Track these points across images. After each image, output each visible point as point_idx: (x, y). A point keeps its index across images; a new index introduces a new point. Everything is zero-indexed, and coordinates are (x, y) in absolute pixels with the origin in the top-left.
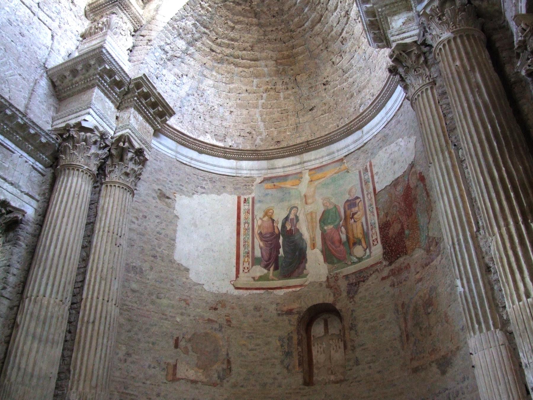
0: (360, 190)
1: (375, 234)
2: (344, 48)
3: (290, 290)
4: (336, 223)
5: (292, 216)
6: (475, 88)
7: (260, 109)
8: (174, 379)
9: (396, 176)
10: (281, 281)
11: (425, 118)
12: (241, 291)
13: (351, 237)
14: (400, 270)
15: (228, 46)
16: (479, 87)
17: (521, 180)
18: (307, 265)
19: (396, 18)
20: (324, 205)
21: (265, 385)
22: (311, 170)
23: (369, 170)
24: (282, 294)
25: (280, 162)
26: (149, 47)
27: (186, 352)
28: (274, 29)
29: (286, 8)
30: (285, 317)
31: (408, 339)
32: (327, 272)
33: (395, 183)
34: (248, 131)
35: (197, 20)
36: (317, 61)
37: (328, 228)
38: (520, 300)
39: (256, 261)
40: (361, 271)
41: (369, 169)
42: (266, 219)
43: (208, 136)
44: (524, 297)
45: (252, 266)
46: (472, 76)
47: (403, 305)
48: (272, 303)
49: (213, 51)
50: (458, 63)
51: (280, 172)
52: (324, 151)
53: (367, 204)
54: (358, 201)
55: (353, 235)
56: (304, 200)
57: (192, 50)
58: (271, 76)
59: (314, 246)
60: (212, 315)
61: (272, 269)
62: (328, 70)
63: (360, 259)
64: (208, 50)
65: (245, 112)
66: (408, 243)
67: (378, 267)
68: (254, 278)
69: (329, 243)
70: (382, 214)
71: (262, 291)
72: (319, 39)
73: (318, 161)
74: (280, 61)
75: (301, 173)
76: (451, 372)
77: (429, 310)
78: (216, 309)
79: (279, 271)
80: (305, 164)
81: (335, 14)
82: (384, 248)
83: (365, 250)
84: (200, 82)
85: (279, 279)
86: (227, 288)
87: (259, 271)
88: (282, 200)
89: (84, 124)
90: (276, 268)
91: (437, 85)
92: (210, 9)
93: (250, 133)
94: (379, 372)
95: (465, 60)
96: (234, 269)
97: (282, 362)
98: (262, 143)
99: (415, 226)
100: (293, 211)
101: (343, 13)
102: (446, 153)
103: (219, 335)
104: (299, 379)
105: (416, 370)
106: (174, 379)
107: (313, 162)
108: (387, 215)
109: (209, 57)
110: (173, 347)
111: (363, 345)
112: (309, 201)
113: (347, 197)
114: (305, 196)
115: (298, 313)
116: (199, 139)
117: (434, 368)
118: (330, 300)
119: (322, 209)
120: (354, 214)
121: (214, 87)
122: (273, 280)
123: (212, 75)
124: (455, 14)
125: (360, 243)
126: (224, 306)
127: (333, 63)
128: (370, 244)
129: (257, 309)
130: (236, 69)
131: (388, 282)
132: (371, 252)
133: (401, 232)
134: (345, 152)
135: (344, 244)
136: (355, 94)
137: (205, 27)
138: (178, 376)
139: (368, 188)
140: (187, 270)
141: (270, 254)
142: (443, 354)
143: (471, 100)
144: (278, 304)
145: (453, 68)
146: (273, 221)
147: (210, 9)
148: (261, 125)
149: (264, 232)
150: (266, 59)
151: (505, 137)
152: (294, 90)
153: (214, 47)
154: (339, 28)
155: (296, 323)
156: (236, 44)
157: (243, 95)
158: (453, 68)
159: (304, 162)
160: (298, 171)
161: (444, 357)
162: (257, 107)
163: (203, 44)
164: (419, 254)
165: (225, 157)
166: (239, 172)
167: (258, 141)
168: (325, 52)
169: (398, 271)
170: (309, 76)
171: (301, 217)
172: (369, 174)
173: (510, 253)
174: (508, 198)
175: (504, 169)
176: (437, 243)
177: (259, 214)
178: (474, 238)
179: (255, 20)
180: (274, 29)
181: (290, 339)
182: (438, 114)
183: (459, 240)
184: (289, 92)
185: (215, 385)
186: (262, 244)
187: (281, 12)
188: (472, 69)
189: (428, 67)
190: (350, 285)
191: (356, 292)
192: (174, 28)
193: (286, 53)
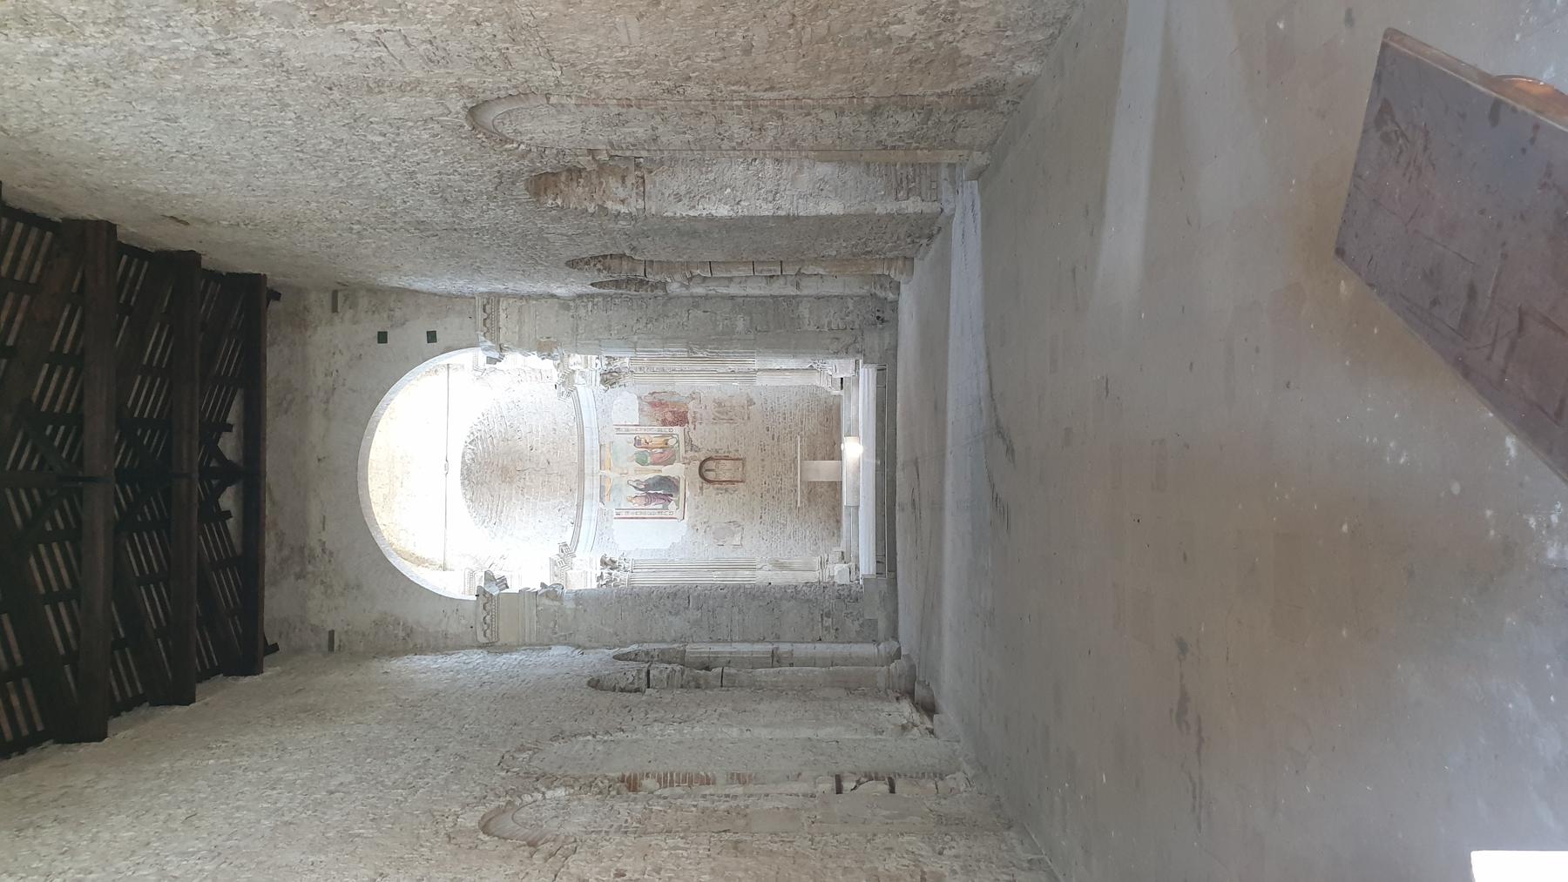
0: (629, 436)
1: (666, 429)
5: (635, 484)
8: (741, 545)
13: (660, 446)
14: (694, 418)
15: (491, 513)
19: (576, 381)
20: (632, 461)
21: (744, 504)
25: (587, 491)
33: (641, 410)
36: (513, 450)
42: (634, 502)
47: (714, 419)
60: (701, 532)
63: (678, 442)
64: (495, 526)
70: (655, 423)
76: (755, 400)
87: (672, 506)
88: (620, 490)
89: (599, 575)
90: (672, 496)
93: (559, 510)
99: (675, 404)
103: (713, 527)
104: (741, 484)
112: (625, 472)
117: (750, 408)
118: (698, 463)
131: (698, 426)
139: (632, 430)
164: (691, 405)
177: (630, 505)
181: (717, 489)
184: (527, 479)
185: (743, 529)
187: (480, 463)
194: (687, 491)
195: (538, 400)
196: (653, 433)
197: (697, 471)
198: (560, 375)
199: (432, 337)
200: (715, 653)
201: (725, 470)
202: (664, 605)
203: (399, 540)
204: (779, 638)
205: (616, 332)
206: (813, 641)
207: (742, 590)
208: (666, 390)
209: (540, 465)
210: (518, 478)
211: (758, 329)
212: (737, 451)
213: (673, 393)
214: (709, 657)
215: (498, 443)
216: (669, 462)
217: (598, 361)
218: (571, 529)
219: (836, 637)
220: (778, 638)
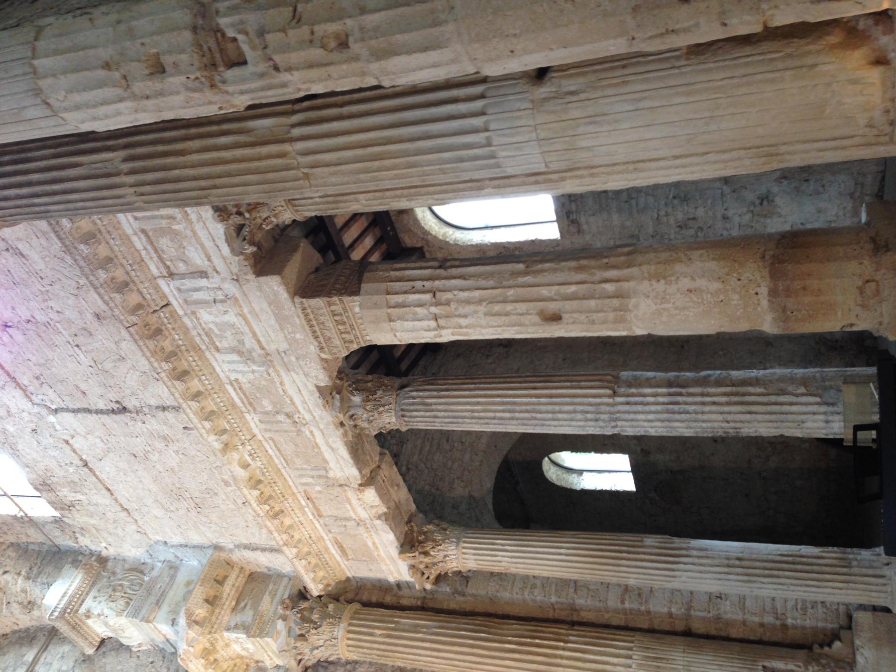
6: (415, 629)
16: (418, 626)
46: (402, 627)
50: (378, 632)
175: (510, 638)
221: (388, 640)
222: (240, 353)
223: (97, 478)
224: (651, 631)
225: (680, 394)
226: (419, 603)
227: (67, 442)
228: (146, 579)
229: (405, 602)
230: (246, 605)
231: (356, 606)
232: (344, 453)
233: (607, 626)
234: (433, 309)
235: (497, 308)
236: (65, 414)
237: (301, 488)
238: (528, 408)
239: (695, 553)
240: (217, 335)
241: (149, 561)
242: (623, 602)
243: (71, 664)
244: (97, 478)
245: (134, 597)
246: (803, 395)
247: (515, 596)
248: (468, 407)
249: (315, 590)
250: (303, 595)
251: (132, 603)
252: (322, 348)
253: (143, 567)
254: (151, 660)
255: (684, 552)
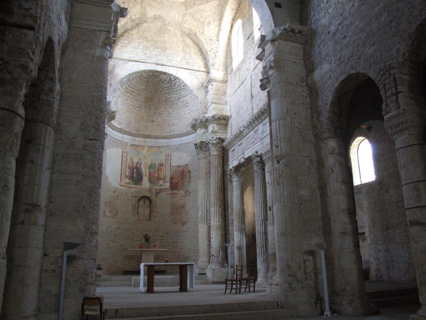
0: (165, 161)
1: (168, 179)
2: (172, 106)
3: (137, 189)
4: (155, 170)
5: (139, 162)
6: (218, 172)
7: (134, 114)
8: (105, 216)
9: (180, 164)
10: (134, 186)
11: (202, 166)
12: (121, 187)
13: (159, 177)
14: (174, 194)
15: (132, 88)
17: (221, 198)
18: (143, 181)
19: (202, 129)
22: (148, 146)
23: (170, 156)
24: (134, 190)
25: (138, 139)
26: (111, 88)
27: (107, 207)
28: (151, 88)
29: (159, 85)
30: (134, 198)
31: (173, 214)
32: (149, 186)
33: (179, 166)
34: (128, 122)
35: (128, 79)
37: (152, 171)
38: (215, 223)
39: (127, 177)
40: (161, 189)
41: (169, 155)
42: (131, 161)
43: (116, 123)
44: (216, 223)
45: (126, 178)
47: (174, 204)
48: (130, 192)
49: (126, 88)
50: (216, 163)
51: (137, 143)
52: (154, 140)
53: (167, 168)
54: (163, 165)
55: (160, 176)
56: (144, 157)
57: (121, 87)
58: (141, 102)
59: (146, 175)
60: (113, 194)
61: (131, 180)
62: (163, 109)
63: (161, 185)
64: (125, 88)
65: (129, 114)
66: (179, 187)
67: (167, 190)
68: (125, 183)
69: (151, 176)
70: (172, 174)
71: (128, 188)
72: (165, 98)
73: (151, 144)
74: (147, 98)
75: (144, 146)
77: (182, 209)
78: (114, 192)
79: (133, 181)
80: (146, 143)
81: (175, 95)
82: (170, 185)
83: (163, 183)
84: (118, 99)
85: (133, 185)
86: (117, 185)
87: (127, 180)
90: (133, 180)
91: (207, 159)
92: (134, 77)
94: (162, 221)
95: (218, 163)
96: (120, 179)
97: (132, 213)
98: (132, 129)
100: (140, 161)
101: (178, 97)
102: (205, 180)
105: (174, 223)
106: (105, 216)
107: (149, 143)
108: (173, 175)
109: (124, 90)
110: (104, 205)
111: (158, 212)
112: (146, 158)
113: (160, 162)
114: (145, 156)
115: (138, 197)
116: (114, 124)
117: (180, 223)
118: (149, 195)
119: (150, 163)
120: (161, 169)
121: (121, 101)
122: (131, 184)
123: (122, 97)
124: (219, 148)
125: (162, 180)
126: (116, 192)
127: (166, 108)
128: (165, 181)
129: (126, 194)
130: (131, 96)
131: (169, 196)
132: (165, 184)
133: (178, 183)
134: (162, 145)
135: (156, 178)
136: (171, 125)
137: (129, 81)
138: (106, 215)
139: (168, 162)
140: (108, 178)
141: (131, 175)
142: (184, 221)
143: (217, 175)
144: (132, 193)
145: (215, 164)
146: (133, 162)
147: (134, 77)
148: (133, 121)
149: (130, 166)
150: (142, 96)
151: (221, 188)
152: (148, 111)
153: (128, 88)
154: (174, 100)
155: (137, 201)
156: (135, 88)
157: (130, 106)
158: (215, 164)
159: (146, 142)
160: (144, 145)
161: (184, 222)
162: (133, 113)
163: (125, 86)
164: (182, 192)
165: (120, 132)
166: (124, 139)
167: (131, 128)
168: (165, 103)
169: (174, 194)
170: (155, 108)
171: (143, 164)
172: (170, 158)
173: (215, 213)
174: (218, 202)
176: (190, 193)
178: (206, 203)
179: (146, 83)
180: (151, 88)
182: (205, 167)
183: (203, 203)
184: (146, 111)
185: (113, 218)
186: (129, 170)
187: (157, 85)
188: (219, 167)
189: (206, 151)
190: (156, 192)
191: (158, 195)
192: (121, 81)
193: (150, 97)
194: (134, 189)
195: (186, 116)
196: (167, 173)
197: (144, 195)
198: (209, 118)
199: (278, 5)
200: (43, 149)
201: (144, 210)
202: (90, 120)
203: (124, 40)
204: (51, 215)
205: (291, 107)
206: (44, 248)
207: (97, 185)
208: (192, 178)
209: (151, 117)
210: (146, 106)
211: (302, 206)
212: (155, 217)
213: (189, 182)
214: (40, 145)
215: (165, 97)
216: (150, 180)
217: (215, 138)
218: (119, 127)
219: (46, 271)
220: (50, 214)
221: (215, 166)
222: (263, 132)
223: (241, 85)
224: (225, 226)
225: (263, 234)
226: (225, 170)
227: (246, 79)
228: (222, 97)
229: (225, 166)
230: (219, 127)
231: (222, 155)
232: (249, 155)
233: (225, 216)
234: (270, 182)
235: (271, 197)
236: (250, 81)
237: (242, 142)
238: (259, 201)
239: (241, 236)
240: (265, 126)
241: (227, 96)
242: (230, 220)
243: (201, 81)
244: (241, 85)
245: (217, 96)
246: (264, 258)
247: (229, 194)
248: (258, 187)
249: (224, 144)
250: (223, 141)
251: (216, 96)
252: (263, 154)
253: (225, 94)
254: (205, 102)
255: (241, 233)
